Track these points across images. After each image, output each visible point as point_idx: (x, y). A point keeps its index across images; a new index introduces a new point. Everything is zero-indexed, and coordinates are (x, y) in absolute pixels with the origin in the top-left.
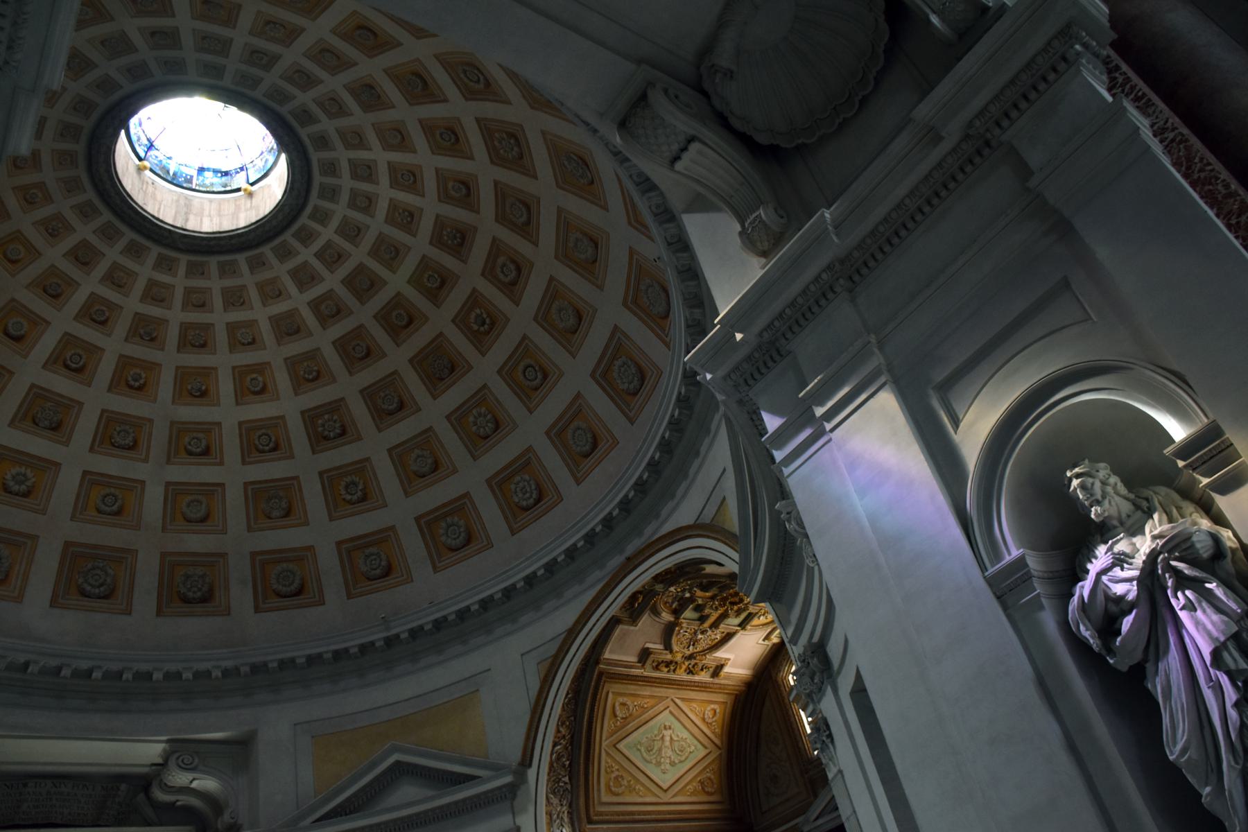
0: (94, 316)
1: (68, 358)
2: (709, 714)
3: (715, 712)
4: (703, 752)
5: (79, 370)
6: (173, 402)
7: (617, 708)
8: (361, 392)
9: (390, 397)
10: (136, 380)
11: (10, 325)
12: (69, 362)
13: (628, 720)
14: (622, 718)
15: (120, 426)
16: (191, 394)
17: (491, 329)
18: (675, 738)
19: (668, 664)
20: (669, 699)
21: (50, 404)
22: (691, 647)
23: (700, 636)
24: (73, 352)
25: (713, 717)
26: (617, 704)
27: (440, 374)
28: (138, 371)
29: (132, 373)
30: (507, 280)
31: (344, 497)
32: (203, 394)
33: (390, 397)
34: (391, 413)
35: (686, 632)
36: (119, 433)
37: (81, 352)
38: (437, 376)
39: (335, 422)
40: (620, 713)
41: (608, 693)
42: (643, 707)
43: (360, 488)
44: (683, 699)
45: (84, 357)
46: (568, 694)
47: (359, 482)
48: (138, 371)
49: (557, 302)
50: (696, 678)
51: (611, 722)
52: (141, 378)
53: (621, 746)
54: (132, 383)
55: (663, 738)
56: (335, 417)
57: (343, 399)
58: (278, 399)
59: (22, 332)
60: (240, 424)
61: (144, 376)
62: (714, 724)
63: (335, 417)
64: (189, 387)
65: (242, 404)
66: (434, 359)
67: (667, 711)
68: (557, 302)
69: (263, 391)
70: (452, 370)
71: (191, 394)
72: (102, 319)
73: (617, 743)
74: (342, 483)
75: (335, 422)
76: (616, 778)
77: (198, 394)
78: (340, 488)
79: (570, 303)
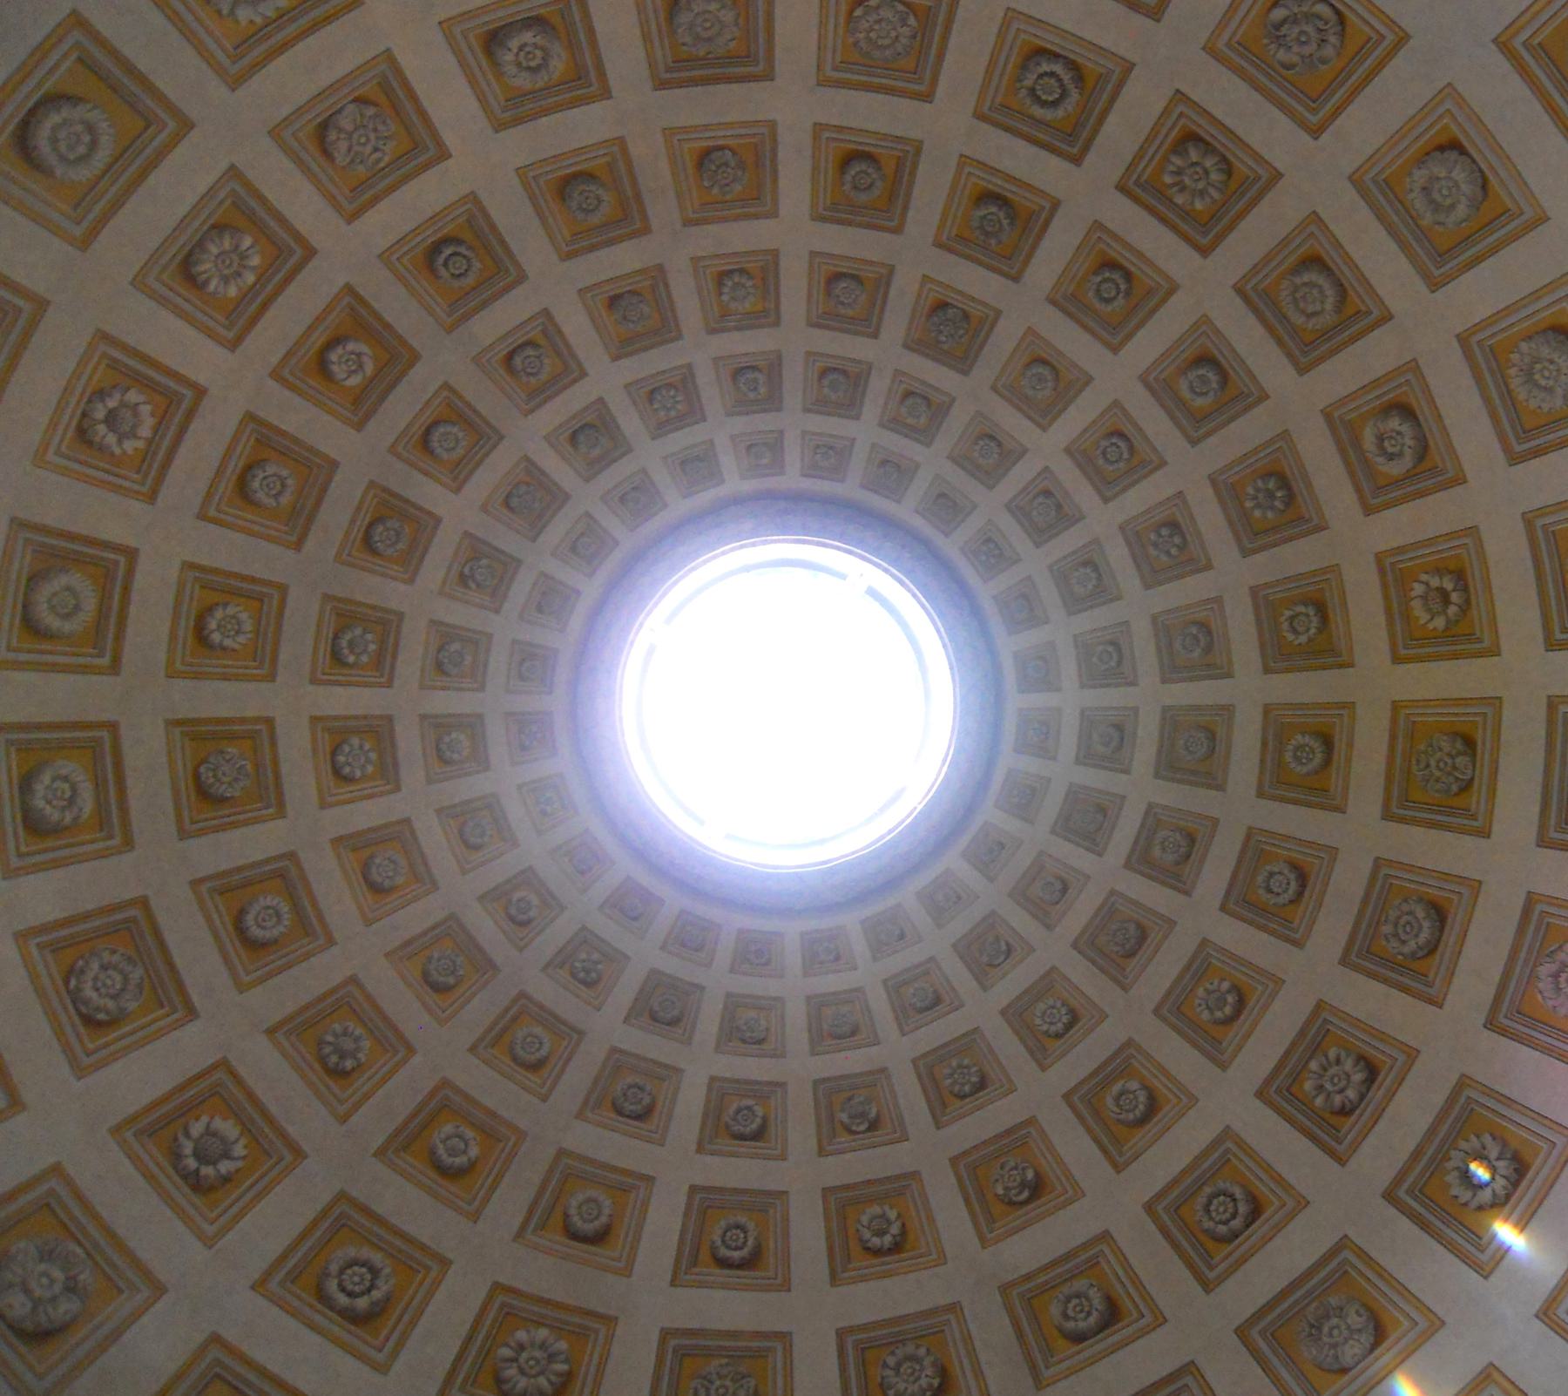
0: (736, 1128)
1: (719, 1243)
5: (752, 1262)
6: (984, 1242)
8: (1344, 961)
9: (1405, 918)
10: (881, 1233)
11: (573, 1211)
12: (724, 1252)
15: (893, 1353)
16: (1011, 1203)
17: (1466, 589)
21: (716, 1362)
24: (723, 1223)
27: (1457, 779)
28: (876, 1209)
29: (865, 1219)
30: (1407, 461)
31: (1474, 1204)
32: (1037, 1188)
33: (1405, 918)
34: (1432, 948)
36: (897, 1372)
37: (742, 1219)
38: (1455, 788)
39: (1338, 1061)
43: (1494, 1154)
45: (751, 1226)
47: (1484, 1148)
48: (876, 1209)
49: (1513, 371)
52: (889, 1222)
54: (876, 1242)
56: (1332, 1054)
57: (1320, 1006)
58: (1193, 1100)
59: (604, 1219)
60: (1149, 1208)
61: (892, 1215)
63: (1332, 1054)
64: (1000, 1191)
65: (1128, 1164)
66: (1422, 765)
68: (1513, 371)
69: (1153, 1106)
70: (1470, 743)
71: (1011, 1203)
72: (754, 1126)
74: (1448, 1178)
75: (1338, 1061)
77: (1026, 1194)
78: (1454, 1191)
79: (1530, 338)
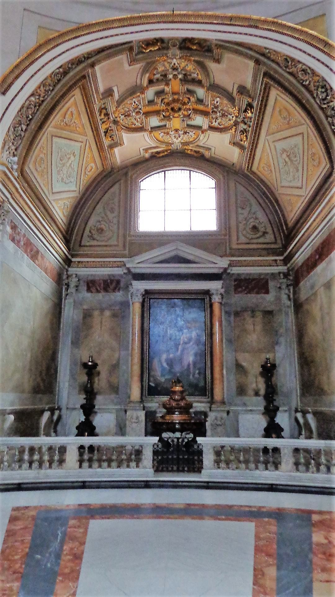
2: (89, 168)
3: (91, 170)
4: (74, 188)
7: (69, 112)
13: (67, 127)
14: (66, 123)
18: (72, 166)
19: (107, 115)
20: (86, 138)
22: (123, 116)
23: (134, 114)
25: (89, 172)
26: (70, 110)
35: (135, 102)
40: (67, 119)
41: (74, 95)
42: (76, 128)
44: (90, 147)
46: (60, 67)
50: (104, 138)
51: (60, 119)
53: (55, 140)
55: (69, 158)
62: (87, 176)
67: (80, 144)
73: (56, 136)
76: (42, 158)
